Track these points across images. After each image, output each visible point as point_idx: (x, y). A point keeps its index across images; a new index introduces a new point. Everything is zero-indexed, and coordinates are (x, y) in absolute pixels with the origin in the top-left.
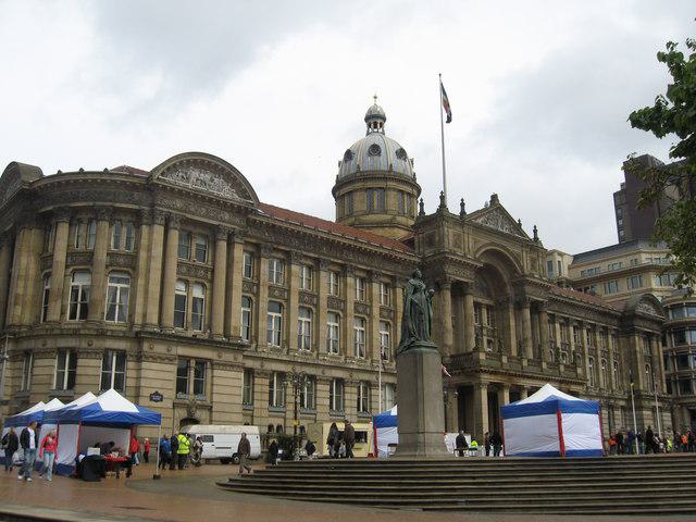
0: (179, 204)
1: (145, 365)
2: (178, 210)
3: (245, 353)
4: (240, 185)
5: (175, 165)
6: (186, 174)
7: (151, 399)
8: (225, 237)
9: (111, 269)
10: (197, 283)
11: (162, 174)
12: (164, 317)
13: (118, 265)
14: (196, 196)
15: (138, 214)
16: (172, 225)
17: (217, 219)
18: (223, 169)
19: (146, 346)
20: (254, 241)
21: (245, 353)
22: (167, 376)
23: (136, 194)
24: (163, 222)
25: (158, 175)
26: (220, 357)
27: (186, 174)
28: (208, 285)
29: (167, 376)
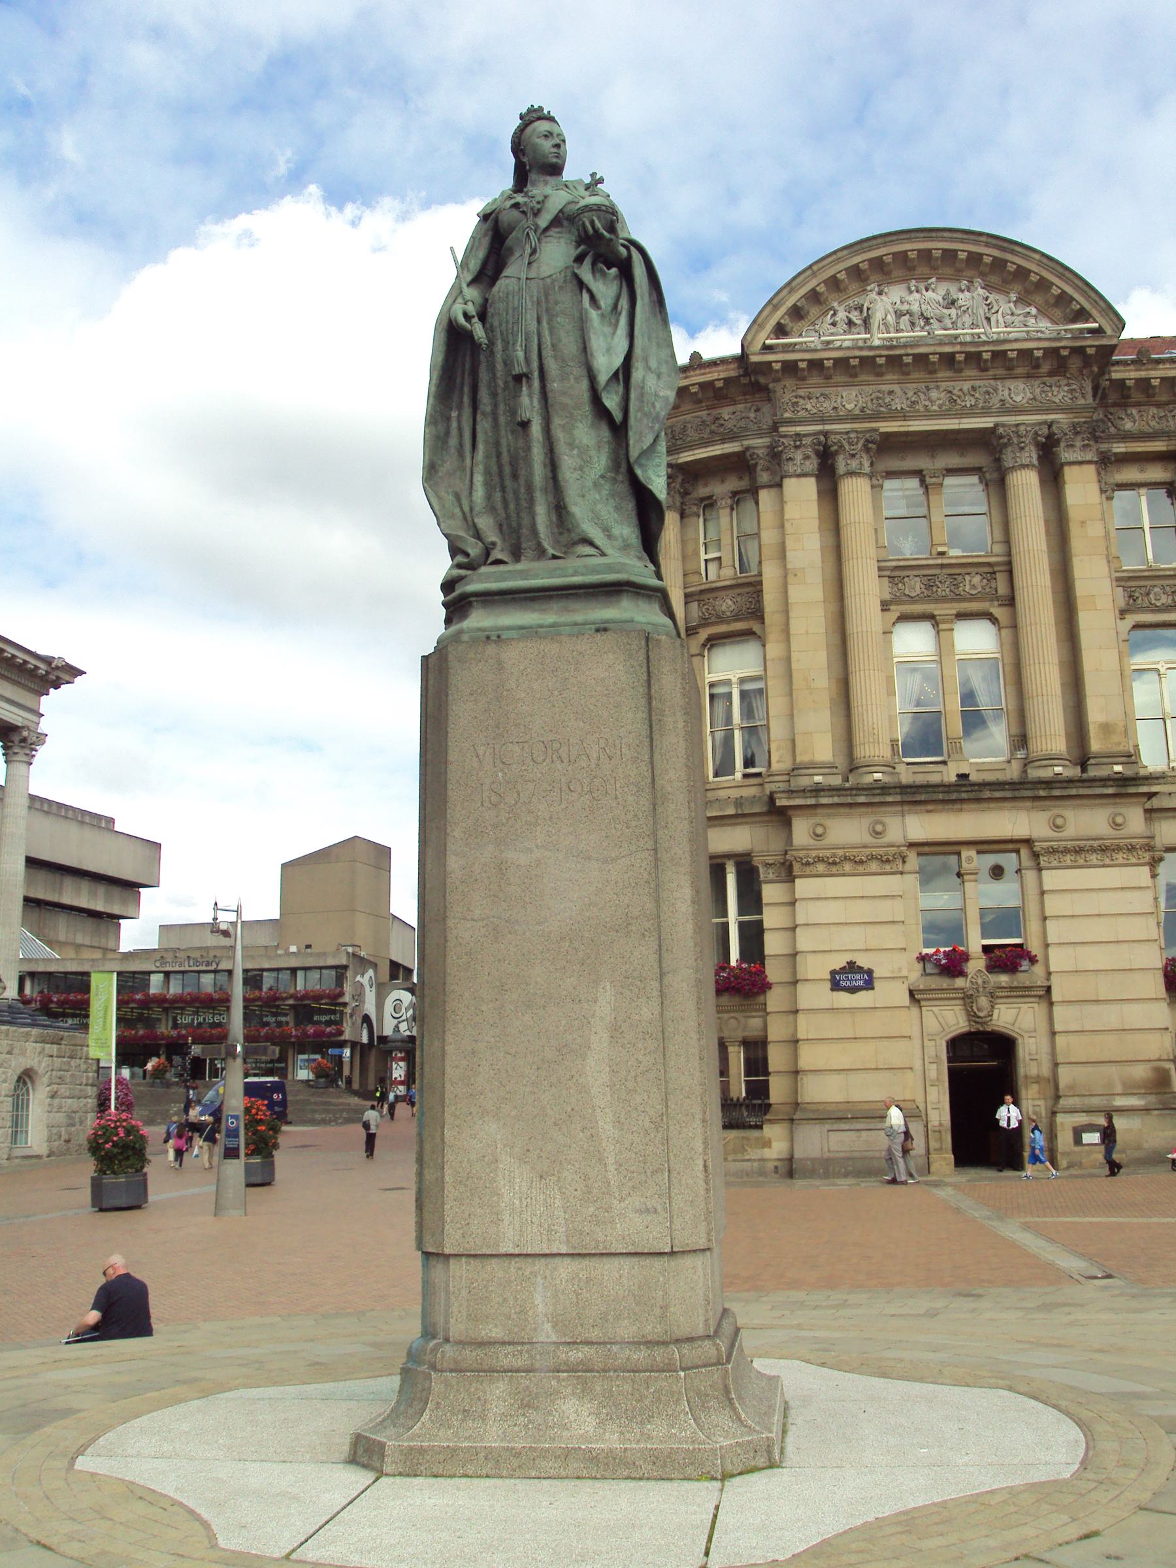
0: (850, 398)
1: (803, 886)
2: (854, 418)
3: (1155, 803)
4: (1043, 285)
5: (814, 296)
6: (860, 308)
7: (836, 986)
8: (1031, 455)
9: (704, 634)
10: (962, 616)
11: (780, 330)
12: (859, 736)
13: (721, 620)
14: (894, 362)
15: (740, 464)
16: (841, 465)
17: (986, 412)
18: (974, 259)
19: (801, 830)
20: (1159, 446)
21: (1155, 803)
22: (886, 910)
23: (725, 412)
24: (812, 465)
25: (764, 337)
26: (1116, 826)
27: (860, 308)
28: (997, 611)
29: (886, 910)
